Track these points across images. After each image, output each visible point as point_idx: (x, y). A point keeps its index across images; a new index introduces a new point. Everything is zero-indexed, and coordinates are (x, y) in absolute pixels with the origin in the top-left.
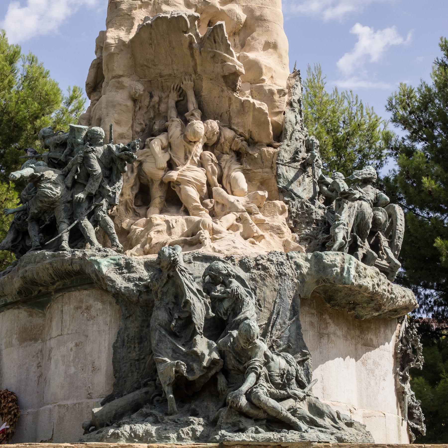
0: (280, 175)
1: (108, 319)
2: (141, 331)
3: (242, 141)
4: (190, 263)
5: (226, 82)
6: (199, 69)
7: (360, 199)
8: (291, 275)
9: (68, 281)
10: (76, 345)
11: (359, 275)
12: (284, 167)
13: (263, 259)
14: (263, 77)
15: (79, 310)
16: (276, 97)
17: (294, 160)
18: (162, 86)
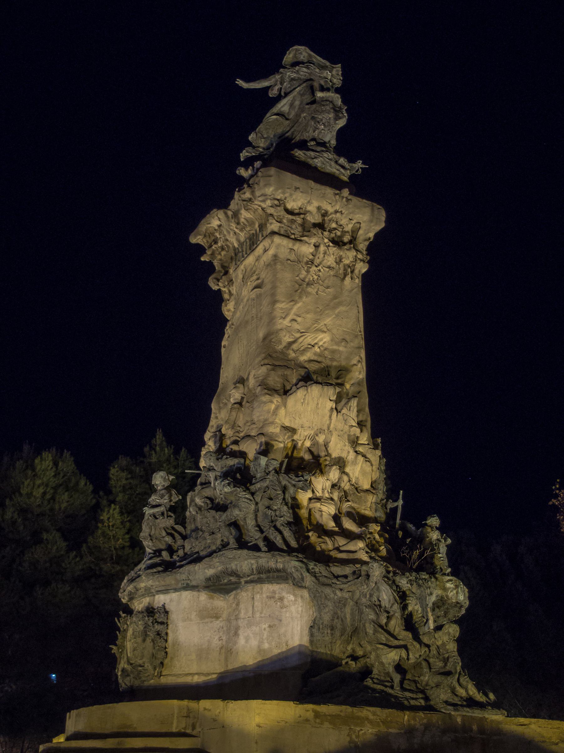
1: (300, 609)
2: (333, 620)
5: (349, 440)
6: (332, 426)
9: (263, 576)
10: (270, 626)
15: (272, 599)
18: (300, 435)
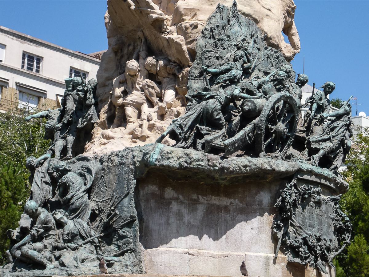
0: (189, 87)
3: (176, 66)
4: (74, 163)
7: (212, 97)
8: (127, 163)
11: (162, 158)
12: (193, 81)
13: (113, 154)
14: (184, 18)
16: (189, 31)
17: (201, 74)
